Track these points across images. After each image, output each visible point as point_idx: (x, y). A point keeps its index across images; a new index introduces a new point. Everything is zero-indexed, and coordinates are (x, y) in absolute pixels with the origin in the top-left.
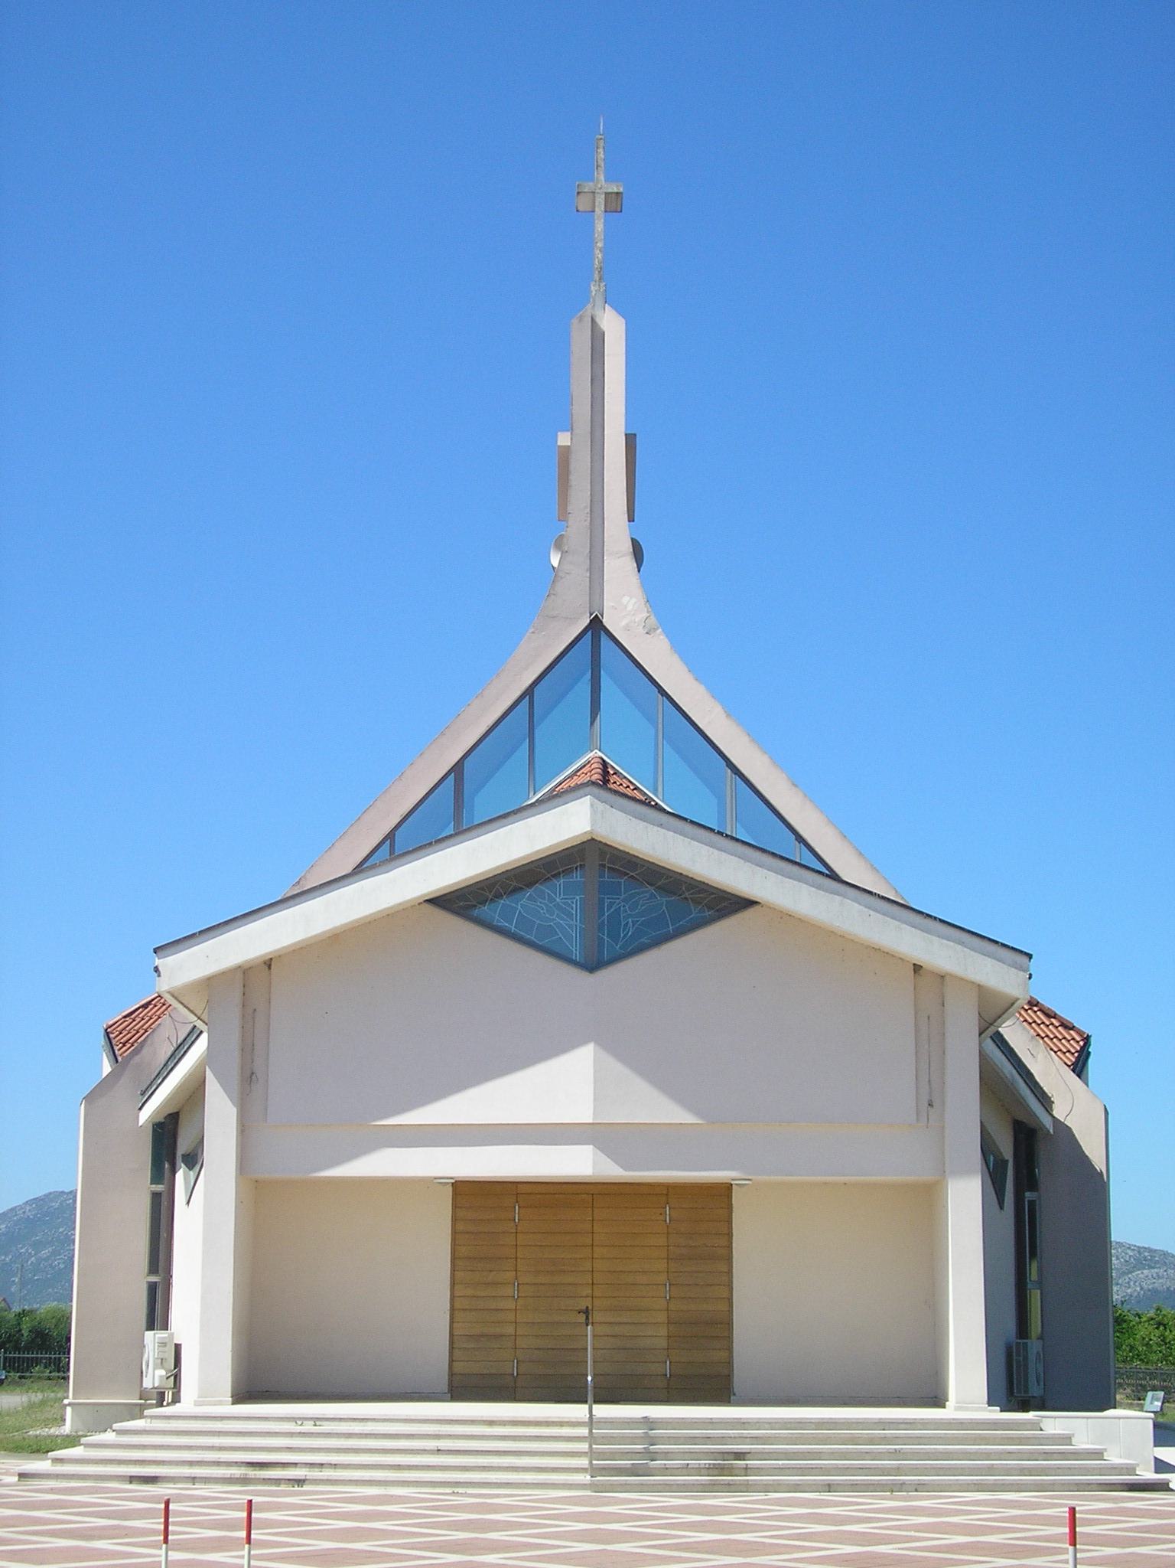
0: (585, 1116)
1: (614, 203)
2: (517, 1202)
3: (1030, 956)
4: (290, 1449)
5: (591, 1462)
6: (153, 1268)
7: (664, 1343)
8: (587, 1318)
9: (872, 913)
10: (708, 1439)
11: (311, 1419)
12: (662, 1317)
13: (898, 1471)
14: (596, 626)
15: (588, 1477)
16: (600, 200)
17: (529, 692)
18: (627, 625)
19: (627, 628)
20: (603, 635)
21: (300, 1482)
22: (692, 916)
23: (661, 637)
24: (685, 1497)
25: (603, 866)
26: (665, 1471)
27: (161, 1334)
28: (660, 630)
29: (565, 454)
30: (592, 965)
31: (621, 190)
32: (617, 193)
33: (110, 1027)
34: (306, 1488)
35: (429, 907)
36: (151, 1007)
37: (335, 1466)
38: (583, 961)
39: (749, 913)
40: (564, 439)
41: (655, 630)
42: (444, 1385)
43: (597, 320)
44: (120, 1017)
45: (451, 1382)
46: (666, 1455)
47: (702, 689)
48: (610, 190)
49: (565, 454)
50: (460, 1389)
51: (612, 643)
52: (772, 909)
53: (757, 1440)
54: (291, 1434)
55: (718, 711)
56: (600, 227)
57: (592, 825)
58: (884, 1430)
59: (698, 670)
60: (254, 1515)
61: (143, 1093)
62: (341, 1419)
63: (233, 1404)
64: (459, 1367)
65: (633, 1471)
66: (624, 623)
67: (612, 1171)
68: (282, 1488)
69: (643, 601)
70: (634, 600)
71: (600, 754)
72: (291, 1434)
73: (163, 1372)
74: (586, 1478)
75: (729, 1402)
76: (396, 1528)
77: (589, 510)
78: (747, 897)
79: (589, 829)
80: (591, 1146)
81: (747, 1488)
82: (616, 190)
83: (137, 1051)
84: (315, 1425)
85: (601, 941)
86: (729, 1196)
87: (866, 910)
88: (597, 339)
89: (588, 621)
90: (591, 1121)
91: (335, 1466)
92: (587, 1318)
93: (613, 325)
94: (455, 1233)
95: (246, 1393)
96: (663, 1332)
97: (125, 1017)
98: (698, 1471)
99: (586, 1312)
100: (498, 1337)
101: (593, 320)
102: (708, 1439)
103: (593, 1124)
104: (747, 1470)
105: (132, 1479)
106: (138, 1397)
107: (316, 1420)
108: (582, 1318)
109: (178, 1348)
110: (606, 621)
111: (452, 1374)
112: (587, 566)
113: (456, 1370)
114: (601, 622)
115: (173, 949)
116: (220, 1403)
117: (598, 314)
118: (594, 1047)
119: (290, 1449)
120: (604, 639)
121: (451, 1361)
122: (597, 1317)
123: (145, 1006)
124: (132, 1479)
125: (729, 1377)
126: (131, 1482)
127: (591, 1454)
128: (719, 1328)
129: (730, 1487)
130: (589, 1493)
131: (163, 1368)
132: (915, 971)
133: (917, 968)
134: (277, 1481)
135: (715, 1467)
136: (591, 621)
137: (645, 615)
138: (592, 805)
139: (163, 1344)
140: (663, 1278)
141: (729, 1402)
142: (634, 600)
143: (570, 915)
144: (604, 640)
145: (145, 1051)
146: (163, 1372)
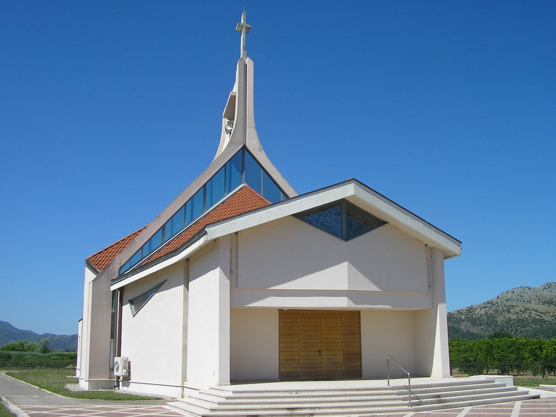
0: (345, 287)
3: (461, 243)
4: (297, 403)
7: (342, 361)
8: (320, 353)
12: (341, 353)
14: (244, 148)
18: (254, 148)
19: (253, 149)
26: (427, 403)
31: (250, 27)
32: (249, 27)
37: (319, 408)
39: (386, 226)
41: (262, 150)
42: (277, 375)
44: (91, 256)
48: (247, 26)
50: (284, 377)
57: (355, 193)
58: (461, 385)
63: (231, 385)
66: (253, 147)
73: (125, 371)
79: (354, 194)
80: (347, 297)
82: (249, 27)
84: (296, 393)
87: (424, 226)
89: (242, 146)
90: (347, 289)
91: (319, 408)
95: (234, 381)
96: (342, 357)
99: (320, 351)
104: (446, 401)
107: (297, 391)
108: (319, 353)
109: (129, 363)
111: (279, 372)
116: (227, 385)
119: (297, 403)
121: (279, 368)
122: (323, 353)
123: (100, 253)
128: (357, 355)
131: (125, 369)
133: (426, 245)
137: (259, 146)
138: (354, 186)
145: (111, 266)
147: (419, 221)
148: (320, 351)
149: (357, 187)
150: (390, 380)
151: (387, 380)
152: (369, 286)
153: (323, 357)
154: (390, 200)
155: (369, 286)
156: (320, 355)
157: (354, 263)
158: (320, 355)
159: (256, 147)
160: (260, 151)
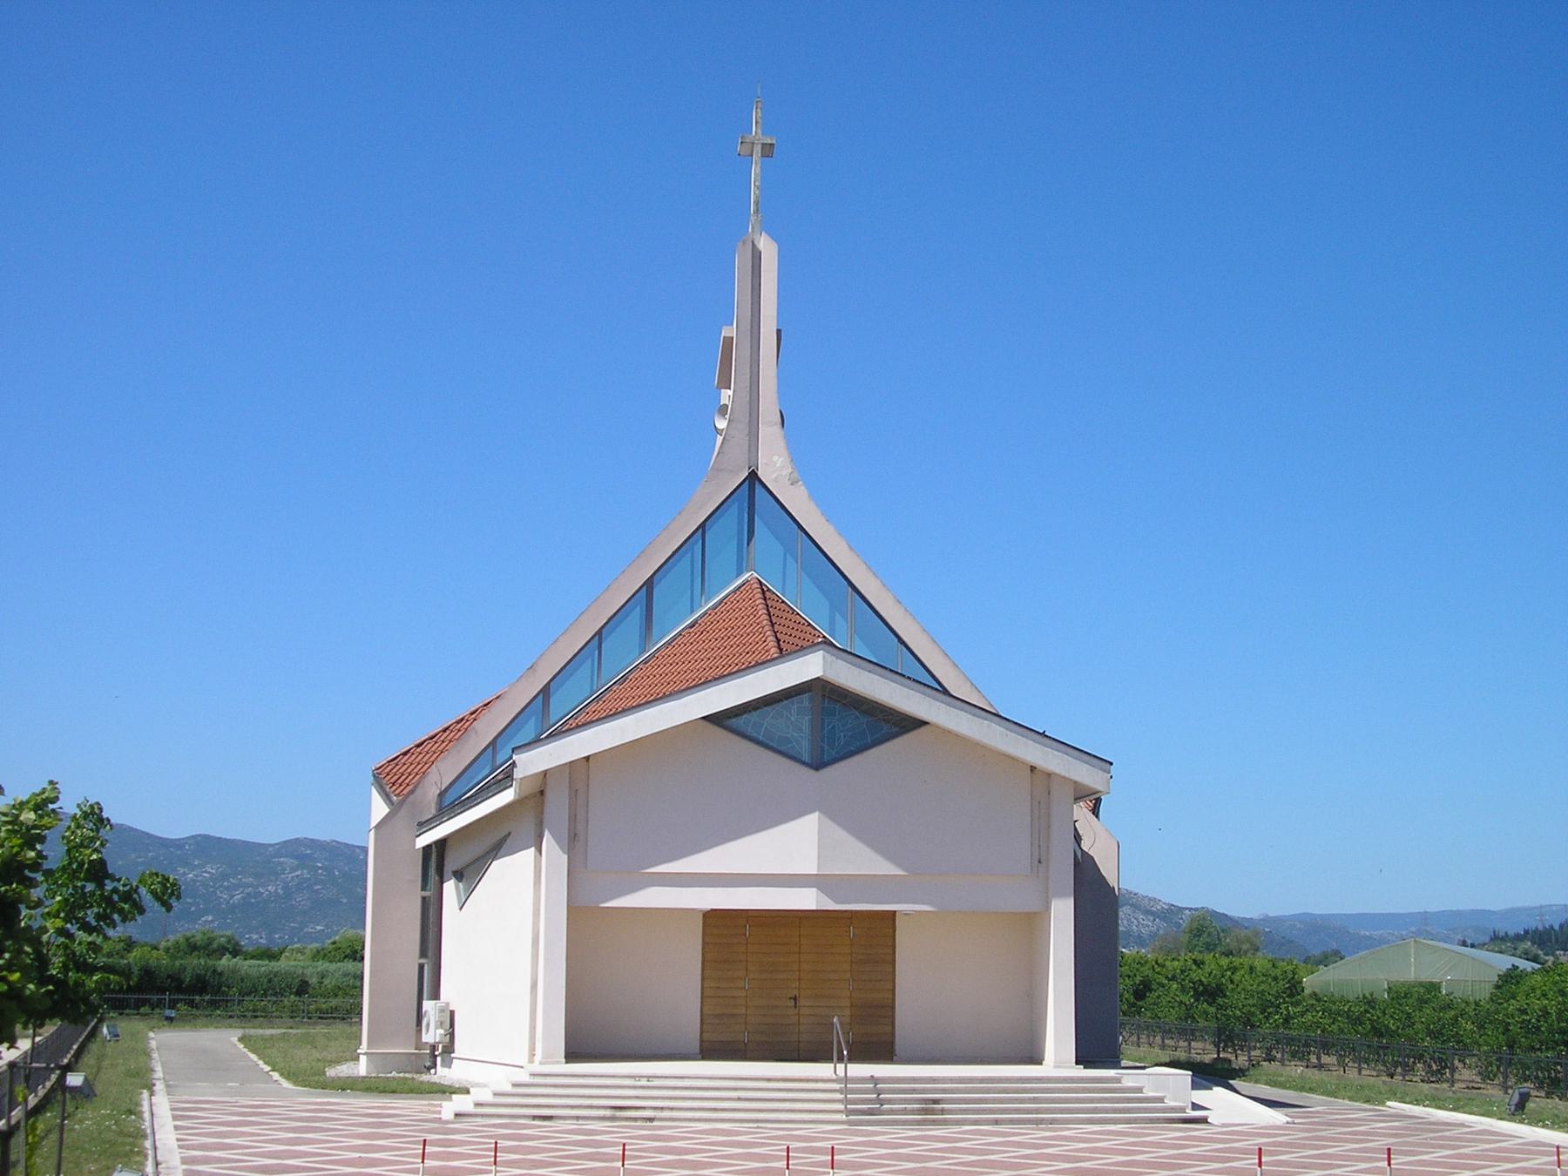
0: (812, 869)
1: (768, 150)
2: (747, 922)
3: (1111, 764)
4: (637, 1097)
5: (846, 1107)
6: (423, 953)
8: (796, 1003)
9: (1008, 733)
10: (914, 1091)
11: (646, 1077)
13: (1038, 1111)
14: (753, 477)
15: (844, 1116)
16: (758, 150)
17: (702, 526)
18: (776, 478)
19: (776, 480)
20: (757, 485)
21: (651, 1120)
22: (883, 732)
23: (802, 488)
24: (917, 1130)
25: (824, 695)
26: (892, 1112)
27: (439, 1004)
28: (800, 483)
29: (728, 342)
30: (818, 765)
31: (774, 142)
32: (771, 144)
33: (378, 769)
34: (655, 1123)
35: (705, 723)
36: (409, 755)
37: (672, 1109)
38: (810, 762)
39: (923, 729)
40: (726, 332)
41: (797, 482)
42: (695, 1046)
43: (756, 243)
44: (385, 762)
45: (701, 1046)
46: (890, 1101)
47: (831, 529)
49: (728, 342)
50: (709, 1052)
51: (764, 490)
52: (938, 727)
53: (945, 1091)
54: (635, 1087)
55: (843, 546)
56: (755, 171)
57: (824, 671)
59: (829, 515)
60: (835, 1158)
61: (421, 824)
62: (666, 1077)
63: (567, 1062)
64: (706, 1036)
65: (870, 1112)
66: (774, 476)
67: (830, 905)
68: (639, 1123)
69: (789, 460)
70: (781, 459)
71: (755, 575)
72: (635, 1087)
73: (442, 1031)
74: (843, 1117)
75: (892, 1060)
76: (945, 1167)
77: (748, 389)
78: (920, 718)
79: (822, 674)
80: (815, 889)
81: (945, 1122)
82: (770, 142)
83: (412, 792)
84: (648, 1081)
85: (822, 747)
86: (894, 920)
87: (1005, 731)
88: (757, 256)
89: (747, 474)
90: (816, 873)
91: (672, 1109)
92: (796, 1003)
93: (768, 247)
94: (704, 944)
95: (572, 1056)
97: (389, 762)
98: (913, 1112)
99: (795, 999)
100: (734, 1015)
101: (753, 243)
102: (914, 1091)
103: (817, 875)
104: (943, 1111)
105: (535, 1117)
106: (414, 1047)
107: (649, 1078)
109: (452, 1013)
110: (759, 473)
111: (702, 1041)
112: (747, 432)
113: (705, 1039)
114: (757, 474)
115: (525, 749)
116: (558, 1063)
117: (756, 237)
119: (637, 1097)
120: (757, 485)
122: (802, 1002)
123: (405, 754)
124: (535, 1117)
125: (892, 1043)
126: (534, 1120)
127: (846, 1101)
128: (885, 1010)
129: (934, 1122)
130: (846, 1127)
131: (442, 1028)
132: (1032, 771)
133: (1033, 768)
134: (635, 1119)
135: (923, 1109)
136: (749, 474)
137: (790, 470)
138: (824, 657)
139: (442, 1011)
140: (848, 976)
141: (892, 1060)
142: (781, 459)
143: (800, 730)
144: (758, 486)
145: (419, 792)
146: (442, 1031)
147: (991, 721)
148: (795, 999)
149: (830, 658)
151: (832, 1065)
153: (804, 1011)
154: (914, 680)
156: (795, 1007)
157: (835, 813)
158: (795, 1007)
159: (784, 474)
160: (792, 484)
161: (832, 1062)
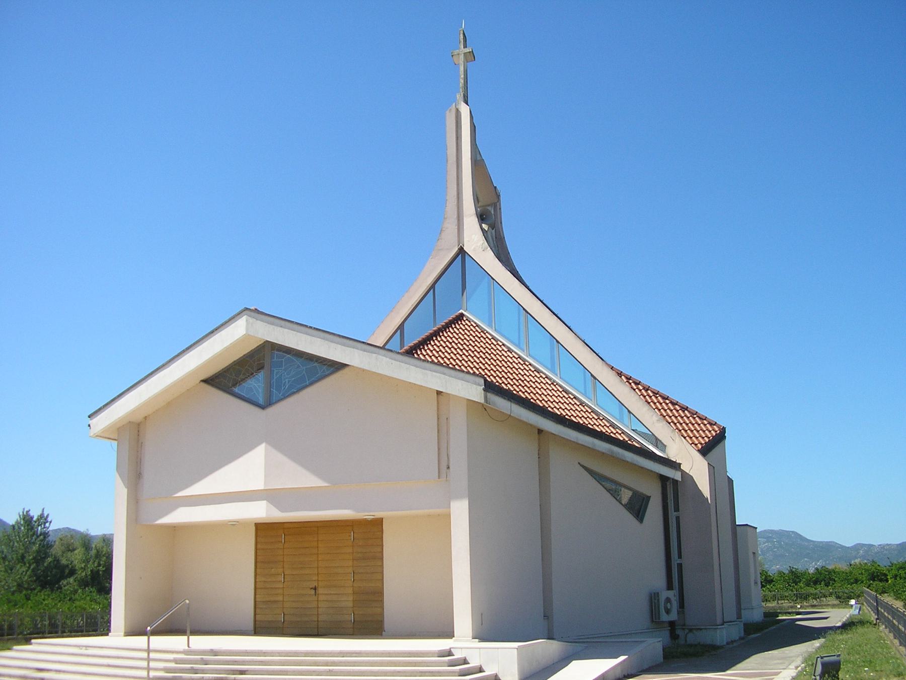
0: (261, 486)
7: (350, 604)
8: (315, 592)
9: (393, 361)
12: (350, 591)
14: (461, 252)
16: (462, 57)
17: (433, 287)
18: (474, 248)
19: (474, 250)
35: (202, 383)
42: (251, 626)
48: (466, 52)
50: (260, 629)
58: (343, 657)
66: (473, 248)
75: (382, 635)
79: (244, 333)
82: (468, 51)
87: (391, 360)
90: (263, 488)
92: (315, 592)
96: (351, 598)
99: (315, 589)
103: (264, 490)
108: (313, 592)
111: (255, 621)
118: (265, 446)
121: (255, 615)
122: (320, 591)
125: (381, 622)
128: (377, 595)
132: (437, 394)
140: (350, 570)
147: (379, 354)
148: (315, 589)
149: (251, 320)
150: (191, 637)
151: (186, 637)
152: (308, 480)
153: (321, 598)
154: (314, 328)
155: (308, 480)
156: (315, 595)
157: (278, 443)
158: (315, 595)
159: (479, 244)
160: (483, 251)
161: (186, 635)
